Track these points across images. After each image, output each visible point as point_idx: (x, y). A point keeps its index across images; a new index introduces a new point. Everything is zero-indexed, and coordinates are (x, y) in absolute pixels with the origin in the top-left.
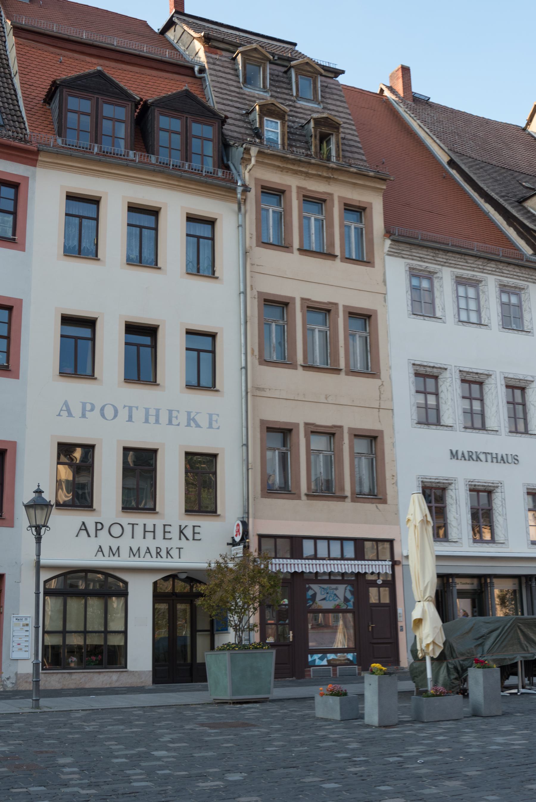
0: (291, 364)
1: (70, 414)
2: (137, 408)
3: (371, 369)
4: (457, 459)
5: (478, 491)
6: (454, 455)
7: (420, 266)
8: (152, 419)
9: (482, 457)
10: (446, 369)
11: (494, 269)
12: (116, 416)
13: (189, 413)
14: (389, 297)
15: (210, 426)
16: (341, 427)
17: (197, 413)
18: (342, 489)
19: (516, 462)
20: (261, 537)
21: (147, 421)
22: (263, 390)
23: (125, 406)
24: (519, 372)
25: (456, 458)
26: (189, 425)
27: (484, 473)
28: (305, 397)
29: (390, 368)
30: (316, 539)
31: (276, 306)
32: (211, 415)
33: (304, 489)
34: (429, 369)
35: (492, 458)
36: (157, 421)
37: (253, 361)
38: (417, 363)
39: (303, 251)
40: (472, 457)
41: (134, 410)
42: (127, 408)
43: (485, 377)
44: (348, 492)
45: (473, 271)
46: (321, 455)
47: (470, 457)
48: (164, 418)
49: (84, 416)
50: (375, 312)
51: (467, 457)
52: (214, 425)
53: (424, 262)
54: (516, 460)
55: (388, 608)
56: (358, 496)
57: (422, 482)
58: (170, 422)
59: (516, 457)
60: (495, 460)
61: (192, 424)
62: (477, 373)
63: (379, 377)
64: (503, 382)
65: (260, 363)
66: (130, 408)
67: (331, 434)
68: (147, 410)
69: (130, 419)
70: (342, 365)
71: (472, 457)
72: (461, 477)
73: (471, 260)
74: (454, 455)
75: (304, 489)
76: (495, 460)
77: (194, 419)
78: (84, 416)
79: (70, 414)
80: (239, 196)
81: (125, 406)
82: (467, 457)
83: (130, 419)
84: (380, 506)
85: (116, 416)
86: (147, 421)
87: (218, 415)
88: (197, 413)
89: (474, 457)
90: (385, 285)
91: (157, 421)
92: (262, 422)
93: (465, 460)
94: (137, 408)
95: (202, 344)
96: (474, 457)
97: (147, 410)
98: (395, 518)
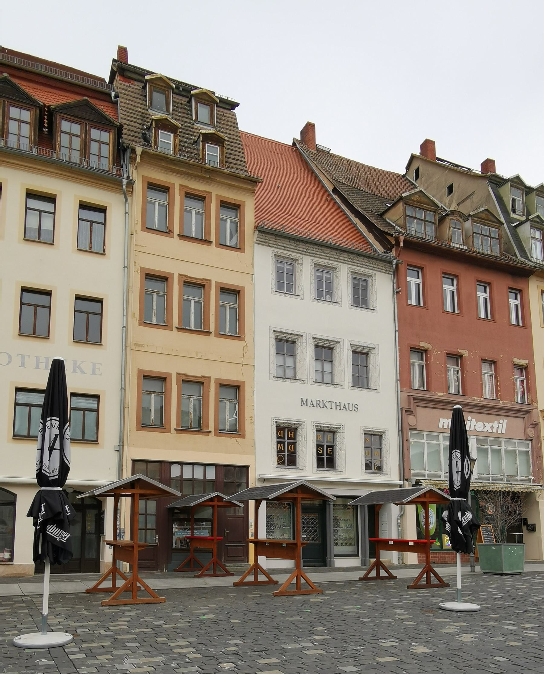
0: (166, 325)
2: (29, 356)
3: (238, 334)
4: (307, 406)
5: (324, 431)
6: (304, 403)
7: (285, 254)
9: (328, 405)
10: (302, 336)
11: (346, 259)
12: (9, 362)
13: (75, 362)
14: (256, 276)
15: (94, 373)
16: (209, 378)
17: (82, 362)
18: (208, 426)
19: (356, 410)
20: (134, 461)
21: (37, 367)
22: (142, 345)
23: (18, 355)
24: (363, 341)
25: (306, 404)
27: (328, 418)
28: (178, 353)
29: (254, 332)
30: (181, 464)
31: (155, 278)
32: (94, 364)
33: (174, 424)
34: (287, 336)
35: (336, 406)
37: (134, 322)
38: (276, 330)
39: (181, 236)
40: (319, 405)
41: (26, 357)
42: (20, 357)
43: (335, 343)
44: (212, 428)
45: (329, 260)
46: (192, 399)
47: (318, 405)
50: (244, 288)
52: (97, 372)
53: (288, 251)
54: (356, 408)
55: (242, 519)
56: (220, 432)
57: (276, 422)
59: (356, 406)
60: (338, 408)
62: (328, 340)
63: (244, 340)
64: (350, 348)
65: (140, 324)
66: (23, 356)
67: (200, 383)
68: (38, 358)
69: (23, 365)
70: (212, 329)
71: (319, 405)
73: (327, 251)
74: (304, 403)
75: (174, 424)
76: (338, 408)
77: (79, 367)
80: (124, 187)
81: (18, 355)
82: (315, 405)
83: (23, 365)
84: (239, 440)
85: (9, 362)
86: (37, 367)
87: (101, 364)
88: (82, 362)
89: (321, 405)
90: (253, 267)
92: (139, 371)
93: (313, 406)
94: (29, 356)
95: (89, 308)
96: (321, 405)
97: (38, 358)
98: (251, 450)
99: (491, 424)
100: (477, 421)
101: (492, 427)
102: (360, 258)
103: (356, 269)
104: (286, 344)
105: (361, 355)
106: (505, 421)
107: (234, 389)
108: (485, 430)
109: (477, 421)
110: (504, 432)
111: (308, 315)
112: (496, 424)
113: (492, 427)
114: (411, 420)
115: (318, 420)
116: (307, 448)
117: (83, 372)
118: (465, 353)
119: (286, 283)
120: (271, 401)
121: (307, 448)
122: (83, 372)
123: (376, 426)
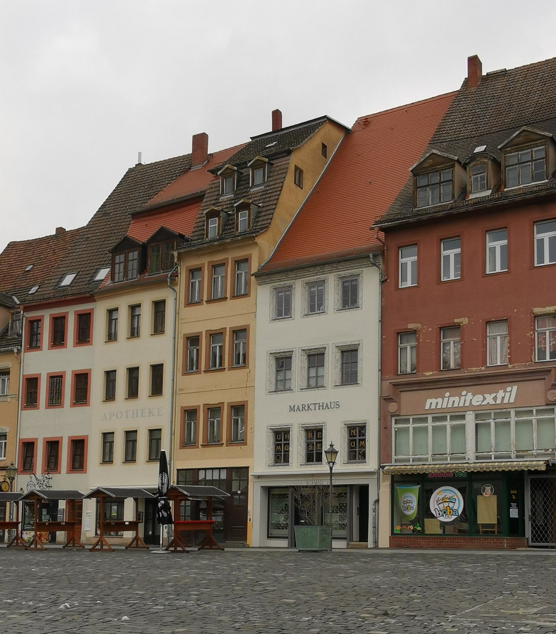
1: (106, 419)
6: (292, 409)
8: (135, 415)
13: (150, 410)
19: (338, 406)
26: (149, 416)
27: (312, 419)
36: (137, 416)
40: (306, 408)
48: (140, 414)
49: (110, 419)
51: (301, 409)
54: (338, 405)
58: (142, 416)
60: (321, 408)
61: (151, 415)
71: (306, 408)
72: (296, 424)
74: (292, 409)
76: (321, 408)
77: (152, 413)
78: (110, 419)
79: (106, 419)
82: (301, 409)
89: (306, 408)
91: (137, 416)
99: (494, 395)
100: (474, 395)
101: (495, 399)
102: (342, 264)
103: (342, 273)
104: (283, 362)
105: (350, 354)
106: (515, 388)
107: (239, 409)
108: (485, 403)
109: (474, 395)
110: (512, 401)
111: (301, 332)
112: (501, 394)
113: (495, 399)
114: (392, 407)
115: (303, 422)
116: (297, 447)
117: (153, 415)
118: (465, 321)
119: (283, 310)
120: (268, 411)
121: (297, 447)
122: (153, 415)
123: (356, 418)
